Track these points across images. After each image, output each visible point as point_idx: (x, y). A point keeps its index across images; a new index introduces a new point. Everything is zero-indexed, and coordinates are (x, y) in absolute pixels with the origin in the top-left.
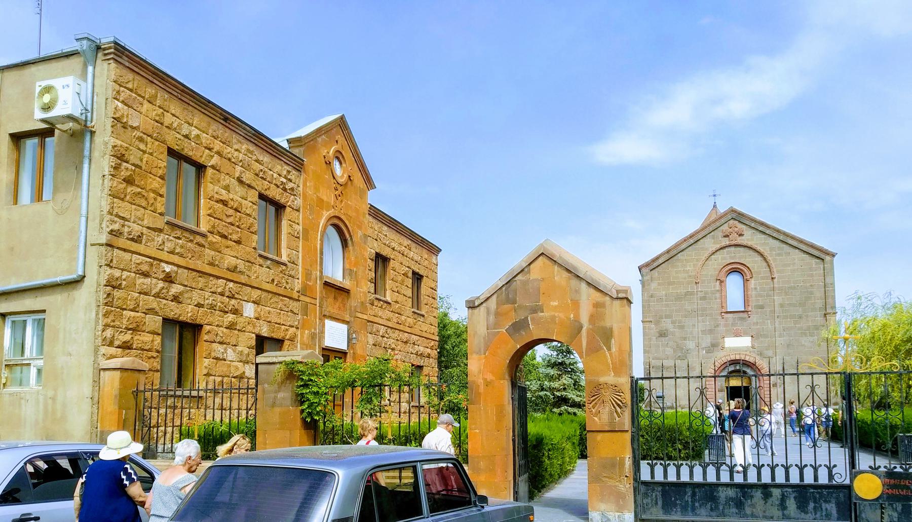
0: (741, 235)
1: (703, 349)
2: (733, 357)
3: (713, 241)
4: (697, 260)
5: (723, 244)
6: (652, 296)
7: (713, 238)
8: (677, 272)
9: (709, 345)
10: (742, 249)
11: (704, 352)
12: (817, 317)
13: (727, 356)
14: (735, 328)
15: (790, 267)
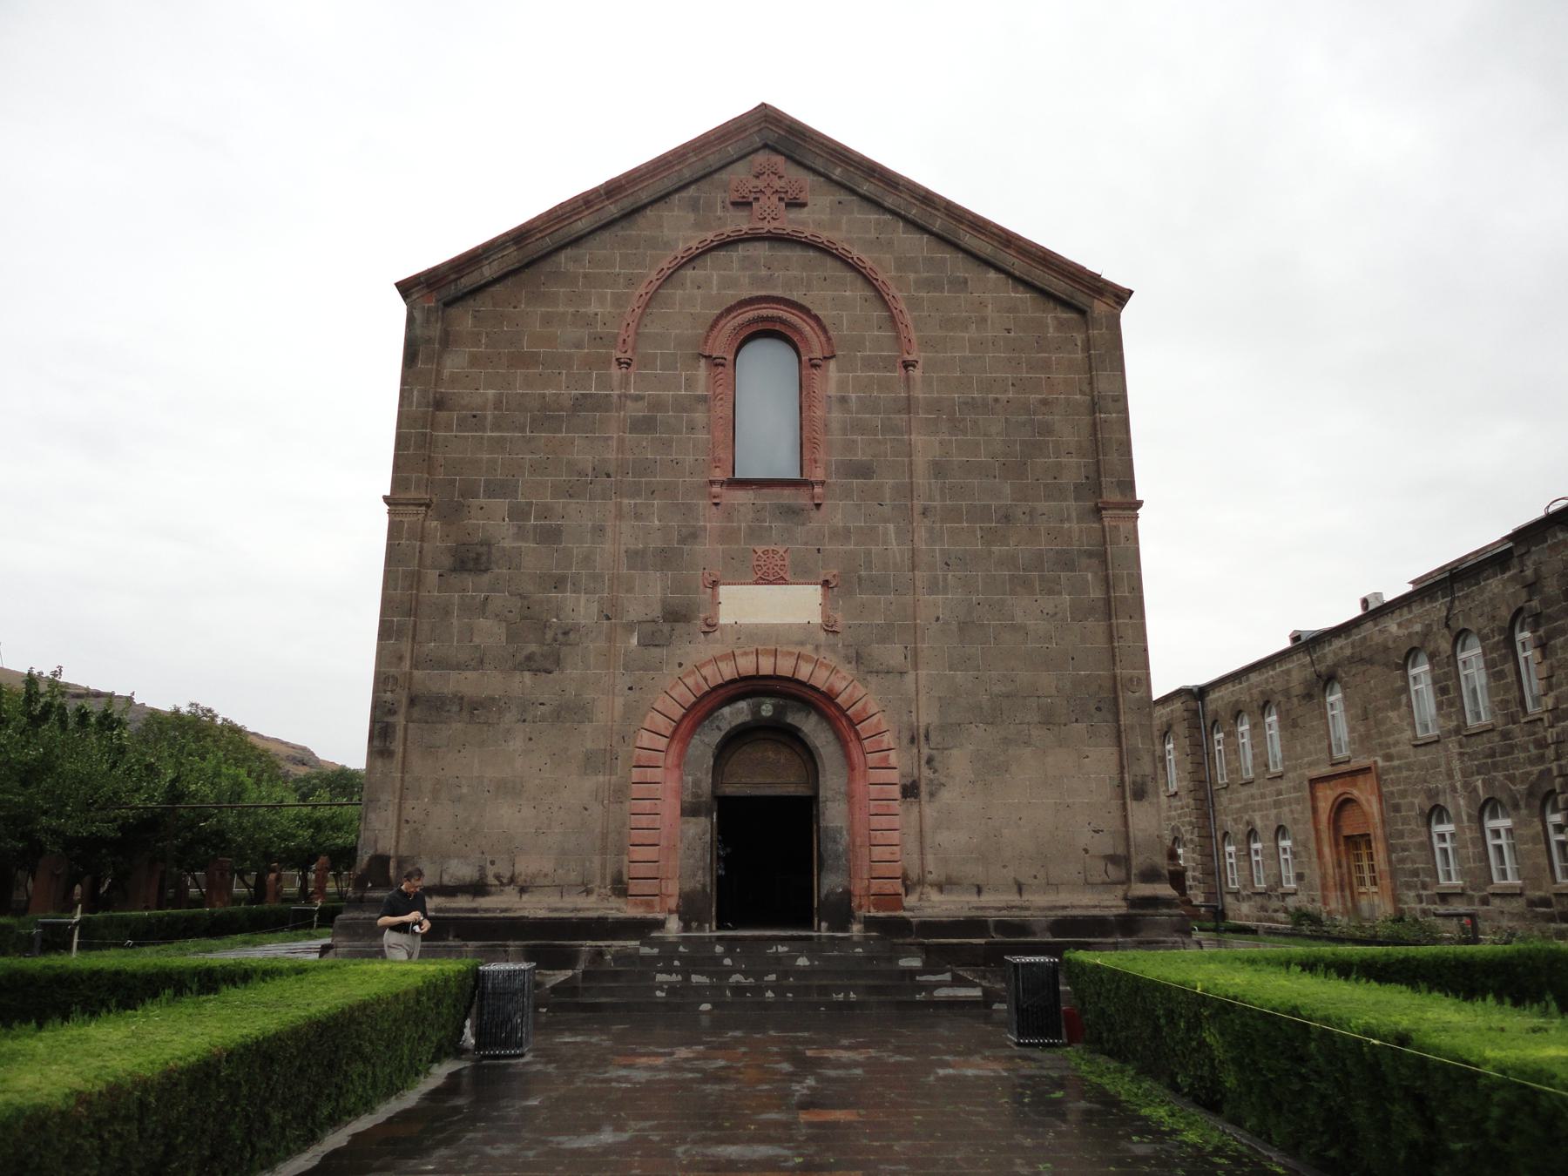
0: (796, 204)
1: (630, 627)
2: (746, 666)
3: (692, 217)
4: (631, 281)
5: (728, 230)
6: (440, 404)
7: (694, 205)
8: (547, 320)
9: (657, 612)
10: (796, 254)
11: (634, 641)
12: (1069, 519)
13: (724, 657)
14: (760, 549)
15: (966, 329)
